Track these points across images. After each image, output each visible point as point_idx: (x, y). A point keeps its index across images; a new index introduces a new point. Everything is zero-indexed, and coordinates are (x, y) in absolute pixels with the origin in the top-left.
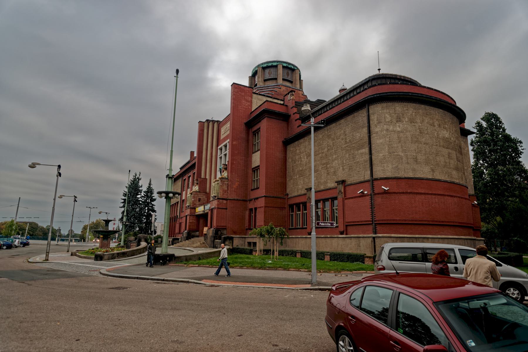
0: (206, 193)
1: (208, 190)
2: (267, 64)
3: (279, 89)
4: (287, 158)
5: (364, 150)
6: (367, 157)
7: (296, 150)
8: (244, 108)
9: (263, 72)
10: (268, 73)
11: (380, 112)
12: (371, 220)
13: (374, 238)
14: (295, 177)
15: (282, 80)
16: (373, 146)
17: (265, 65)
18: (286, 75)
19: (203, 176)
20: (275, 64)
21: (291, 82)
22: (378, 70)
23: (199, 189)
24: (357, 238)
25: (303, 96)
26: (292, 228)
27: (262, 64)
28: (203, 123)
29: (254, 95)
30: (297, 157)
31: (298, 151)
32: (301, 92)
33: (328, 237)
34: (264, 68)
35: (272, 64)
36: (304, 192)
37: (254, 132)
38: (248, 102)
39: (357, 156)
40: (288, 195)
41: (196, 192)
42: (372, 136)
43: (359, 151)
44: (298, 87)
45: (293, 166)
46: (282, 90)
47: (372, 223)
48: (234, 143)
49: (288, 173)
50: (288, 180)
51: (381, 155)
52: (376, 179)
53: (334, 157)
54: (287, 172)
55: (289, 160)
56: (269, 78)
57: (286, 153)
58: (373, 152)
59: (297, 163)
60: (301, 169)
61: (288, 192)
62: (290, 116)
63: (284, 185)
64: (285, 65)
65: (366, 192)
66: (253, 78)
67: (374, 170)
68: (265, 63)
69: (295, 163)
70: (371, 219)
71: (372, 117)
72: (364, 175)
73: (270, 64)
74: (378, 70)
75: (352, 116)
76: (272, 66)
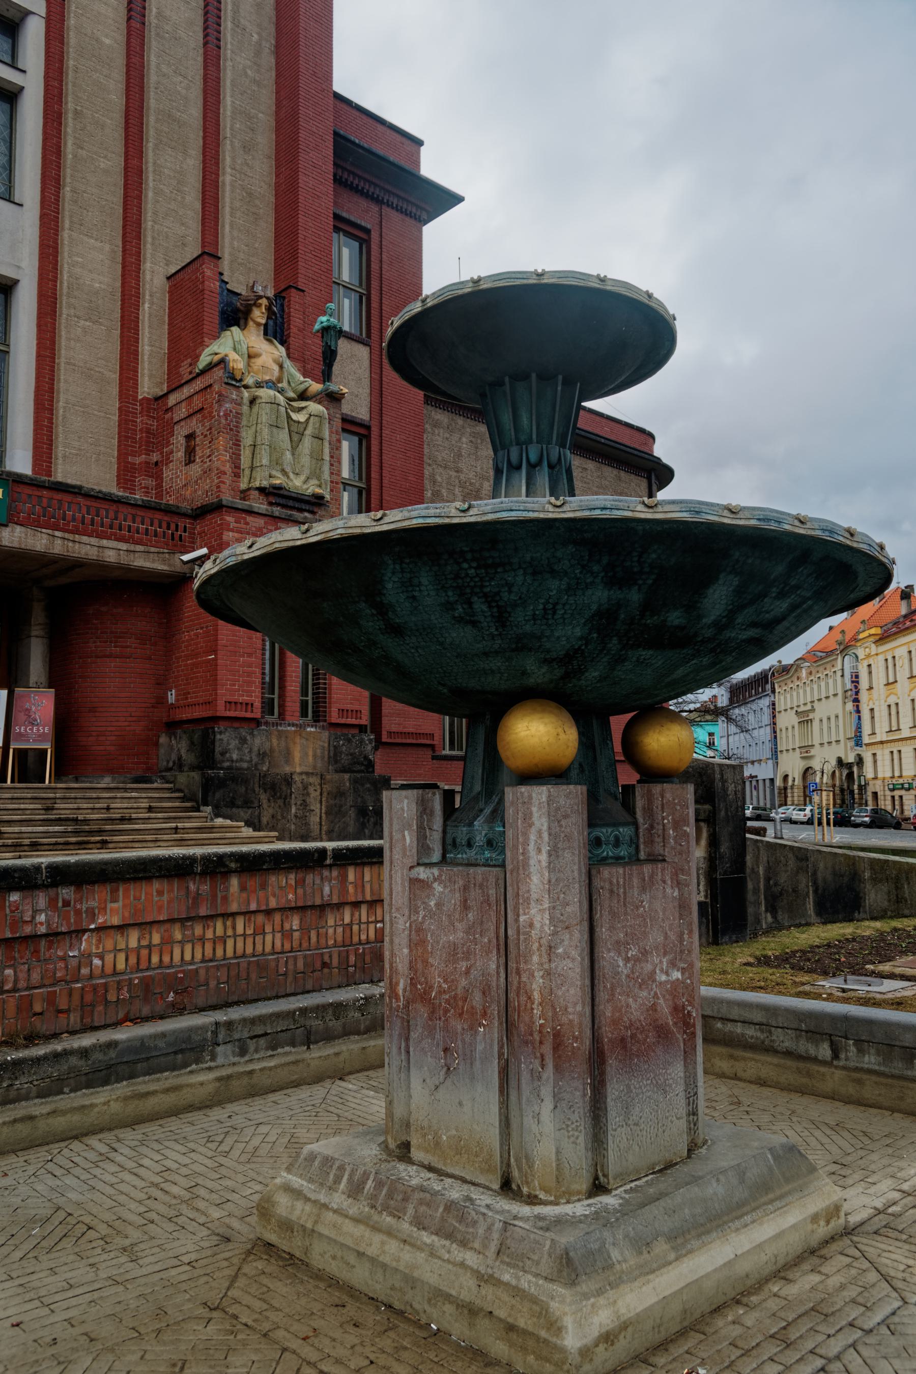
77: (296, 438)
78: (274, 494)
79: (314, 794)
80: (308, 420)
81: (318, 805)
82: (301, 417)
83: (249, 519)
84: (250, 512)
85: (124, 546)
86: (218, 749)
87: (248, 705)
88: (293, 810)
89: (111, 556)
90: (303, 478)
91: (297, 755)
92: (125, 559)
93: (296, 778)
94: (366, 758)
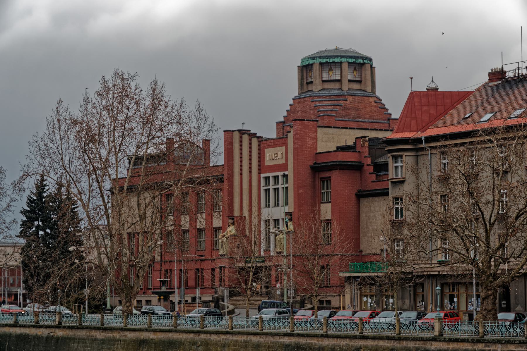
2: (327, 60)
3: (345, 102)
4: (361, 212)
7: (371, 206)
8: (309, 148)
9: (321, 69)
14: (370, 235)
15: (347, 81)
17: (324, 61)
19: (237, 213)
20: (337, 60)
21: (360, 82)
25: (375, 104)
28: (231, 132)
29: (319, 130)
30: (372, 215)
31: (372, 208)
32: (372, 100)
35: (334, 60)
36: (379, 252)
37: (321, 178)
38: (313, 139)
40: (362, 252)
44: (369, 89)
45: (367, 223)
46: (348, 102)
48: (301, 191)
49: (362, 228)
50: (361, 235)
54: (361, 227)
55: (363, 215)
59: (371, 220)
60: (375, 227)
61: (362, 247)
62: (363, 166)
63: (357, 242)
64: (351, 60)
69: (369, 220)
73: (331, 60)
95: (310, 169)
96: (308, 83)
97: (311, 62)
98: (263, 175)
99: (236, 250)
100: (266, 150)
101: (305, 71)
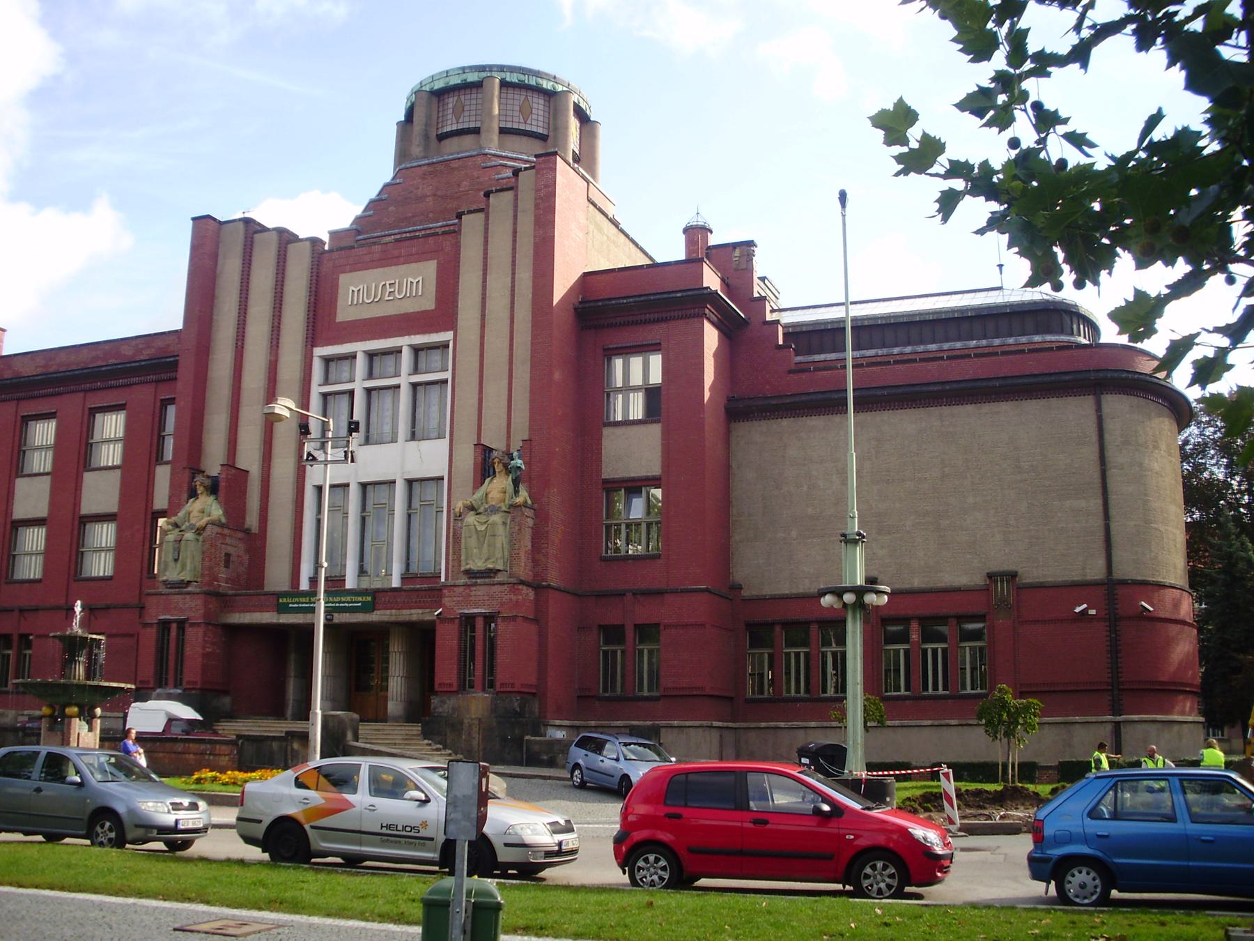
0: (247, 532)
1: (252, 521)
2: (522, 77)
4: (734, 465)
5: (1082, 503)
6: (1098, 522)
10: (517, 108)
11: (1128, 416)
12: (1110, 680)
13: (1117, 724)
14: (781, 535)
16: (1113, 498)
17: (510, 78)
18: (516, 114)
22: (998, 266)
23: (226, 513)
24: (1062, 726)
26: (757, 696)
27: (502, 68)
33: (971, 725)
34: (504, 84)
39: (1059, 515)
41: (221, 525)
42: (1109, 473)
43: (1068, 503)
47: (1110, 688)
51: (1132, 523)
52: (1123, 583)
53: (971, 500)
56: (522, 127)
57: (729, 444)
58: (1113, 512)
63: (724, 555)
65: (1092, 612)
66: (435, 100)
67: (1115, 559)
68: (512, 69)
70: (1109, 678)
71: (1109, 425)
72: (1084, 568)
74: (998, 266)
75: (1042, 402)
76: (538, 90)
77: (482, 539)
78: (469, 573)
79: (475, 729)
80: (487, 528)
81: (477, 736)
82: (483, 528)
83: (455, 589)
84: (455, 586)
85: (420, 611)
86: (432, 706)
87: (451, 685)
88: (464, 737)
89: (414, 618)
90: (483, 560)
91: (473, 708)
92: (421, 617)
93: (466, 721)
94: (514, 710)
95: (572, 310)
96: (442, 137)
97: (472, 77)
98: (320, 351)
99: (223, 574)
100: (344, 278)
101: (435, 106)
